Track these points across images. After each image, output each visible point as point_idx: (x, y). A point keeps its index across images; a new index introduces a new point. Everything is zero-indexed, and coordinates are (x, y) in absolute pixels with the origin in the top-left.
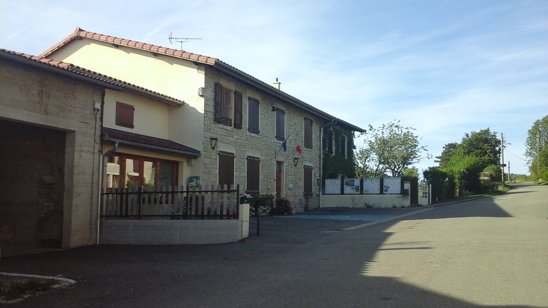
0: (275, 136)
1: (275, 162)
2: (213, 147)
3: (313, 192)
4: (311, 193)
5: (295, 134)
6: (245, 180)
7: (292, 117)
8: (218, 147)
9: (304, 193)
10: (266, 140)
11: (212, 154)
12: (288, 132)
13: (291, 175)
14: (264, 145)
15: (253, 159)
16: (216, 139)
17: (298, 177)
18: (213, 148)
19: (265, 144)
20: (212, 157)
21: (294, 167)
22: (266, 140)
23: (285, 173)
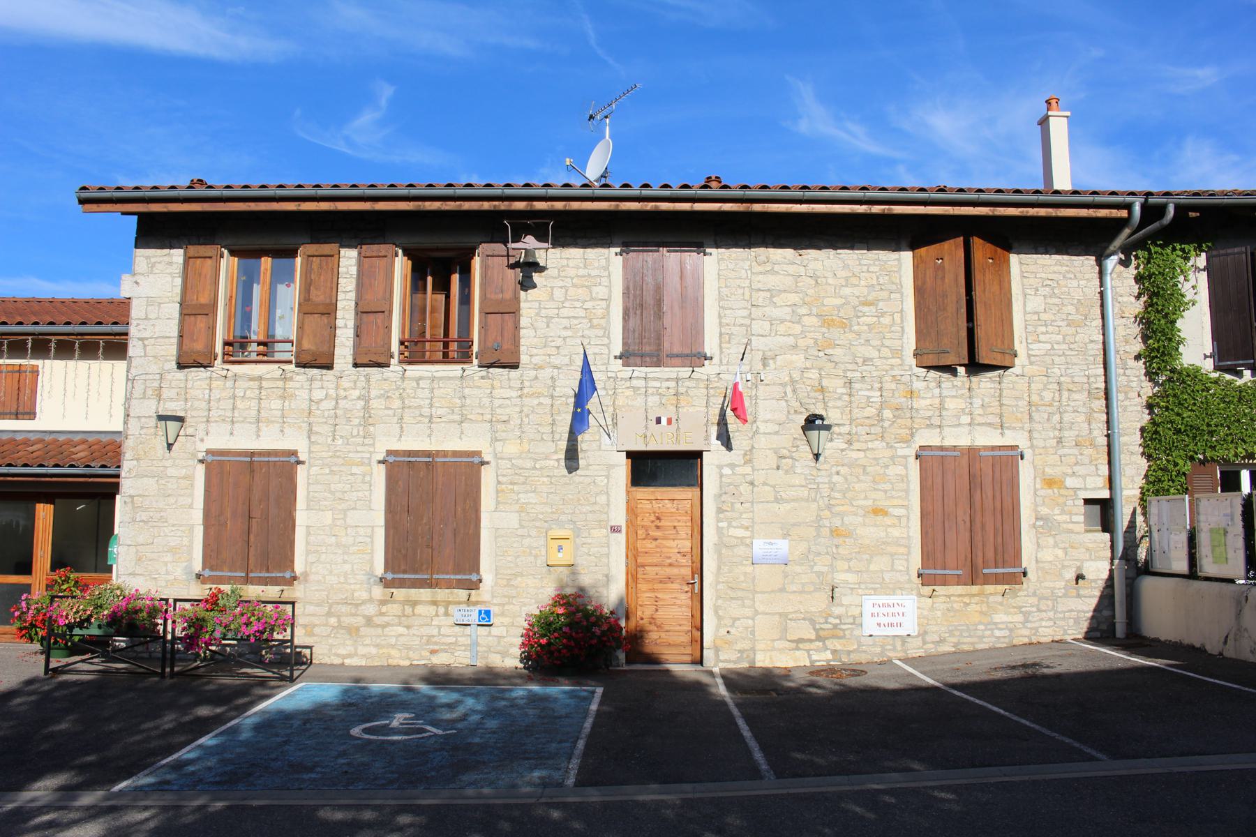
0: (618, 349)
2: (171, 441)
3: (1023, 567)
4: (1019, 570)
5: (811, 321)
6: (371, 537)
8: (202, 440)
9: (919, 575)
10: (536, 378)
11: (168, 463)
12: (747, 321)
13: (778, 500)
15: (428, 460)
16: (181, 419)
17: (861, 503)
18: (170, 446)
20: (170, 472)
22: (536, 378)
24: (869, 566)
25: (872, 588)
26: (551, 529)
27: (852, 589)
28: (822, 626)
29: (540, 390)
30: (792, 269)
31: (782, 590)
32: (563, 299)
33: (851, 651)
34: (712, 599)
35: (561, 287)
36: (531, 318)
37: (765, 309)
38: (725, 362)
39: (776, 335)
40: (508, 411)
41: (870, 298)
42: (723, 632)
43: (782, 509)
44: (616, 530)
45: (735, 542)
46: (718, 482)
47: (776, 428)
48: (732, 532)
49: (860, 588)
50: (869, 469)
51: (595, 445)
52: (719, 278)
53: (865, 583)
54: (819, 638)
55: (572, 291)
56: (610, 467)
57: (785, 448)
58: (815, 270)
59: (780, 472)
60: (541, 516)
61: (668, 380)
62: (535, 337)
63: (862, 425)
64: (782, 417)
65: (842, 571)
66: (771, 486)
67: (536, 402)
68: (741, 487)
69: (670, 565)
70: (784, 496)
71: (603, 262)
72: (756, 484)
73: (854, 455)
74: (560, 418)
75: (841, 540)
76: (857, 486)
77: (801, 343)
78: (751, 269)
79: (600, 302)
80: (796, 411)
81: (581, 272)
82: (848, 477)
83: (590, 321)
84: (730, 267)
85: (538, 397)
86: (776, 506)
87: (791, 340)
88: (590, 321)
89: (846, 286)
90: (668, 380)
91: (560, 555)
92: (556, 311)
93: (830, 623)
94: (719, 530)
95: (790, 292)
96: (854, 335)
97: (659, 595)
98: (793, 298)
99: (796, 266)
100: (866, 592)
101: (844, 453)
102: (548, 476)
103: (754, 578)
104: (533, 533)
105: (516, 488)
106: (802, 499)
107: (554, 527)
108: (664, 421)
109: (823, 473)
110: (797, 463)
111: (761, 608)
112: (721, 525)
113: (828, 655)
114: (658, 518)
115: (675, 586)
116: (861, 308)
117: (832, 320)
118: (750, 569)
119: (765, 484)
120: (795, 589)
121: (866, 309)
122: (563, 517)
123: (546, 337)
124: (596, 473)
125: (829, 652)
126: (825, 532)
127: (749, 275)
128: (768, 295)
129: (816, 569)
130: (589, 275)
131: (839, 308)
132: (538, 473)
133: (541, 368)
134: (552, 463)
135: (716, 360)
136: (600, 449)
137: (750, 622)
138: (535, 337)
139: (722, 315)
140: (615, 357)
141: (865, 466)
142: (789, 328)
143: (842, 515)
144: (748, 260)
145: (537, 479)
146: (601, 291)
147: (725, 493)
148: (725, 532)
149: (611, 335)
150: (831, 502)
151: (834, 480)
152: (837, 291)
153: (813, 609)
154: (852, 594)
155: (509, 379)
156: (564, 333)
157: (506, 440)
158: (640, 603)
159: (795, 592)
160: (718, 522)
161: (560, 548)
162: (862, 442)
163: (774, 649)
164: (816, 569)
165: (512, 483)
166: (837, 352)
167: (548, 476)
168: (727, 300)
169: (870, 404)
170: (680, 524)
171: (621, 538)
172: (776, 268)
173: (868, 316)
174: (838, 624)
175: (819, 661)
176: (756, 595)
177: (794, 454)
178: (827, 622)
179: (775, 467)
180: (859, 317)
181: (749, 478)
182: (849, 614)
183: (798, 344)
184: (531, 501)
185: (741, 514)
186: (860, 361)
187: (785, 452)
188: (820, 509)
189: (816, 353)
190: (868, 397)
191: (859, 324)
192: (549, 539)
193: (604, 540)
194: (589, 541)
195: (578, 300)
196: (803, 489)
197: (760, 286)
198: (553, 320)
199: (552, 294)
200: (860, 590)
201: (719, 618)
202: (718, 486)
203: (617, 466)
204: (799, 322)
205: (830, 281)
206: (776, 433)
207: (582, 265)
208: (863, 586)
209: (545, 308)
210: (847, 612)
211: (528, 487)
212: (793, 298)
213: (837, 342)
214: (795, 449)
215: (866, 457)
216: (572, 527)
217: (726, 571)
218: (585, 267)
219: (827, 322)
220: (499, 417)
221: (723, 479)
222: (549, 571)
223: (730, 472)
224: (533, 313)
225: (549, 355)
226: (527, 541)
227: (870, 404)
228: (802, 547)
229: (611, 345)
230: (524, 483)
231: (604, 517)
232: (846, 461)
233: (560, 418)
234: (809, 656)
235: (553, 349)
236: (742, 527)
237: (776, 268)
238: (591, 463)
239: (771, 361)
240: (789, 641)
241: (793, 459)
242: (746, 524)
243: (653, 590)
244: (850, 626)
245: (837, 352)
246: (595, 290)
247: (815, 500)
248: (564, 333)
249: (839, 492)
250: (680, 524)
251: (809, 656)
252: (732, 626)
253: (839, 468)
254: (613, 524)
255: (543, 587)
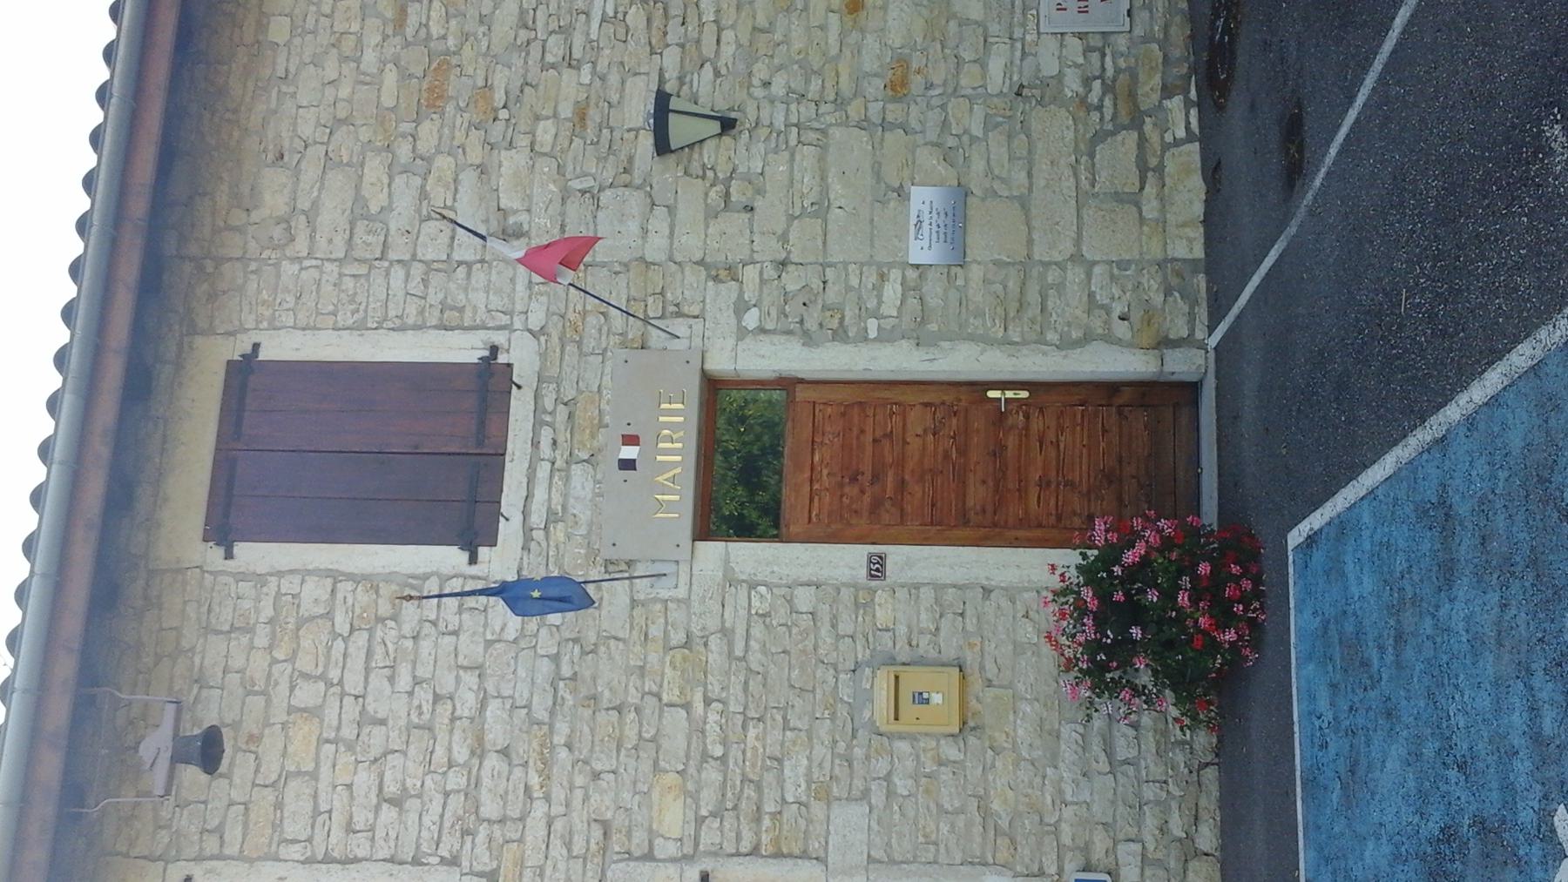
1: (712, 551)
5: (428, 132)
7: (274, 192)
10: (505, 752)
13: (821, 208)
14: (558, 794)
19: (546, 777)
21: (746, 154)
23: (808, 339)
24: (976, 22)
25: (1024, 14)
26: (872, 721)
27: (1024, 54)
28: (1108, 117)
29: (535, 744)
30: (310, 172)
31: (1024, 203)
32: (322, 685)
33: (1165, 56)
34: (1045, 354)
35: (292, 689)
36: (358, 762)
37: (393, 227)
38: (505, 320)
39: (452, 208)
40: (579, 825)
41: (389, 14)
42: (1122, 330)
43: (842, 202)
44: (877, 568)
45: (913, 302)
46: (776, 338)
47: (660, 212)
48: (890, 308)
49: (1023, 39)
50: (761, 21)
51: (676, 614)
52: (315, 328)
53: (1011, 25)
54: (1136, 123)
55: (305, 663)
56: (730, 580)
57: (706, 194)
58: (318, 124)
59: (759, 203)
60: (842, 746)
61: (535, 444)
62: (405, 753)
63: (665, 34)
64: (635, 200)
65: (984, 77)
66: (789, 226)
67: (563, 754)
68: (791, 287)
69: (963, 452)
70: (813, 197)
71: (245, 588)
72: (784, 255)
73: (728, 50)
74: (607, 693)
75: (917, 82)
76: (797, 45)
77: (475, 154)
78: (299, 259)
79: (340, 596)
80: (626, 171)
81: (261, 640)
82: (776, 61)
83: (381, 620)
84: (291, 305)
85: (553, 747)
86: (835, 213)
87: (469, 178)
88: (381, 620)
89: (358, 61)
90: (535, 444)
91: (937, 698)
92: (348, 700)
93: (1101, 100)
94: (885, 337)
95: (361, 177)
96: (468, 45)
97: (1035, 476)
98: (375, 169)
99: (303, 165)
100: (1031, 25)
101: (724, 71)
102: (744, 727)
103: (996, 263)
104: (881, 766)
105: (770, 807)
106: (821, 159)
107: (867, 714)
108: (629, 452)
109: (765, 114)
110: (741, 169)
111: (1068, 247)
112: (873, 334)
113: (1175, 104)
114: (854, 479)
115: (1012, 442)
116: (409, 31)
117: (430, 90)
118: (976, 272)
119: (784, 238)
120: (1024, 174)
121: (412, 21)
122: (845, 693)
123: (410, 727)
124: (743, 613)
125: (1167, 103)
126: (895, 112)
127: (314, 262)
128: (361, 226)
129: (977, 131)
130: (270, 622)
131: (405, 76)
132: (735, 752)
133: (480, 740)
134: (713, 717)
135: (499, 338)
136: (686, 602)
137: (1097, 270)
138: (405, 753)
139: (398, 322)
140: (473, 560)
141: (754, 28)
142: (439, 179)
143: (858, 79)
144: (277, 265)
145: (749, 755)
146: (313, 593)
147: (802, 322)
148: (888, 324)
149: (421, 571)
150: (832, 98)
151: (782, 92)
152: (368, 79)
153: (1070, 135)
154: (1035, 55)
155: (502, 821)
156: (404, 682)
157: (650, 831)
158: (1053, 519)
159: (1030, 175)
160: (866, 339)
161: (921, 699)
162: (700, 33)
163: (1162, 223)
164: (977, 131)
165: (758, 820)
166: (500, 79)
167: (744, 727)
168: (366, 311)
169: (620, 16)
170: (869, 429)
171: (897, 555)
172: (304, 204)
173: (429, 17)
174: (1103, 83)
175: (1188, 123)
176: (1037, 257)
177: (721, 176)
178: (1100, 108)
179: (748, 215)
180: (429, 36)
181: (770, 272)
182: (1081, 60)
183: (478, 161)
184: (802, 770)
185: (849, 288)
186: (524, 35)
187: (715, 195)
188: (845, 123)
189: (500, 125)
190: (603, 20)
191: (444, 37)
192: (895, 728)
193: (902, 594)
194: (902, 630)
195: (329, 649)
196: (798, 157)
197: (340, 241)
198: (370, 709)
199: (304, 710)
200: (1028, 38)
201: (1087, 338)
202: (783, 338)
203: (727, 561)
204: (428, 160)
205: (344, 92)
206: (671, 210)
207: (245, 640)
208: (1018, 33)
209: (338, 728)
210: (1077, 66)
211: (769, 777)
212: (375, 169)
213: (481, 83)
214: (710, 174)
215: (733, 27)
216: (868, 671)
217: (978, 322)
218: (250, 630)
219: (433, 100)
220: (593, 847)
221: (770, 326)
222: (973, 729)
223: (755, 311)
224: (346, 759)
225: (453, 719)
226: (902, 785)
227: (620, 16)
228: (928, 159)
229: (445, 571)
230: (759, 788)
231: (846, 594)
232: (741, 66)
233: (607, 693)
234: (1177, 143)
235: (439, 709)
236: (878, 289)
237: (304, 204)
238: (713, 623)
239: (511, 220)
240: (1142, 188)
241: (731, 177)
242: (874, 279)
243: (1022, 491)
244: (1108, 59)
245: (500, 79)
246: (307, 608)
247: (824, 132)
248: (404, 682)
249: (807, 81)
250: (869, 429)
251: (1177, 143)
252: (1107, 310)
253: (756, 82)
254: (864, 572)
255: (1015, 748)
